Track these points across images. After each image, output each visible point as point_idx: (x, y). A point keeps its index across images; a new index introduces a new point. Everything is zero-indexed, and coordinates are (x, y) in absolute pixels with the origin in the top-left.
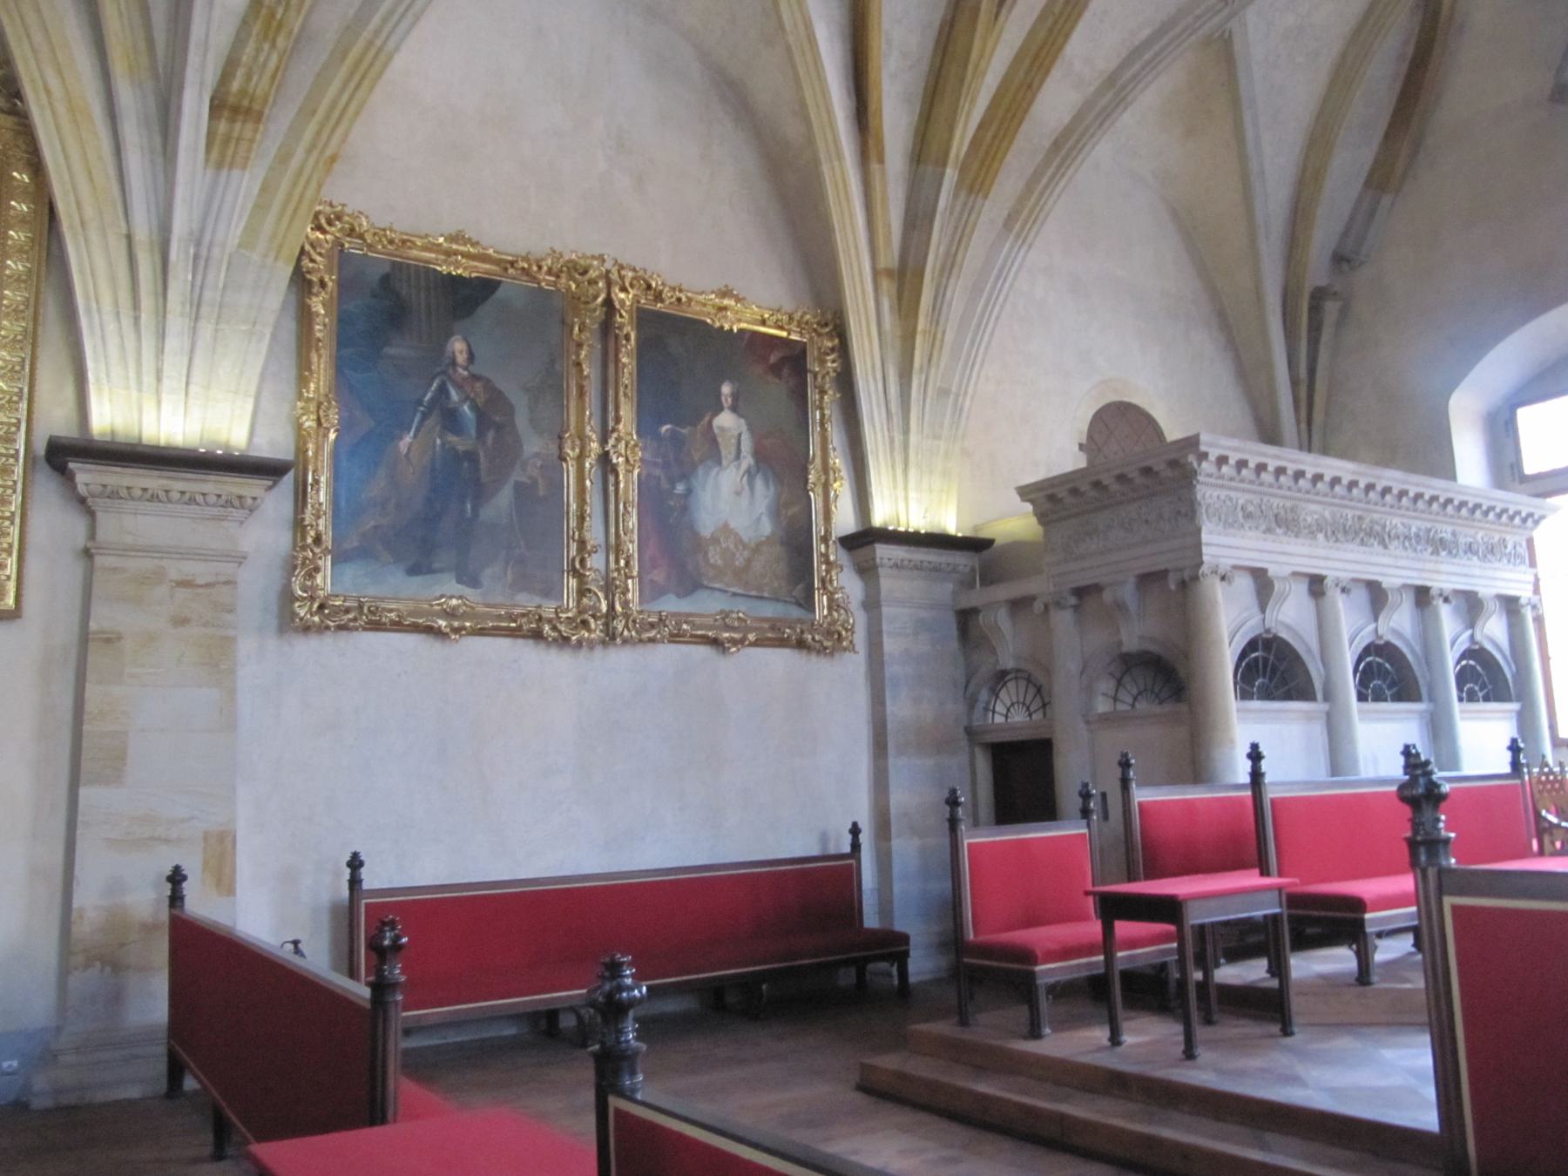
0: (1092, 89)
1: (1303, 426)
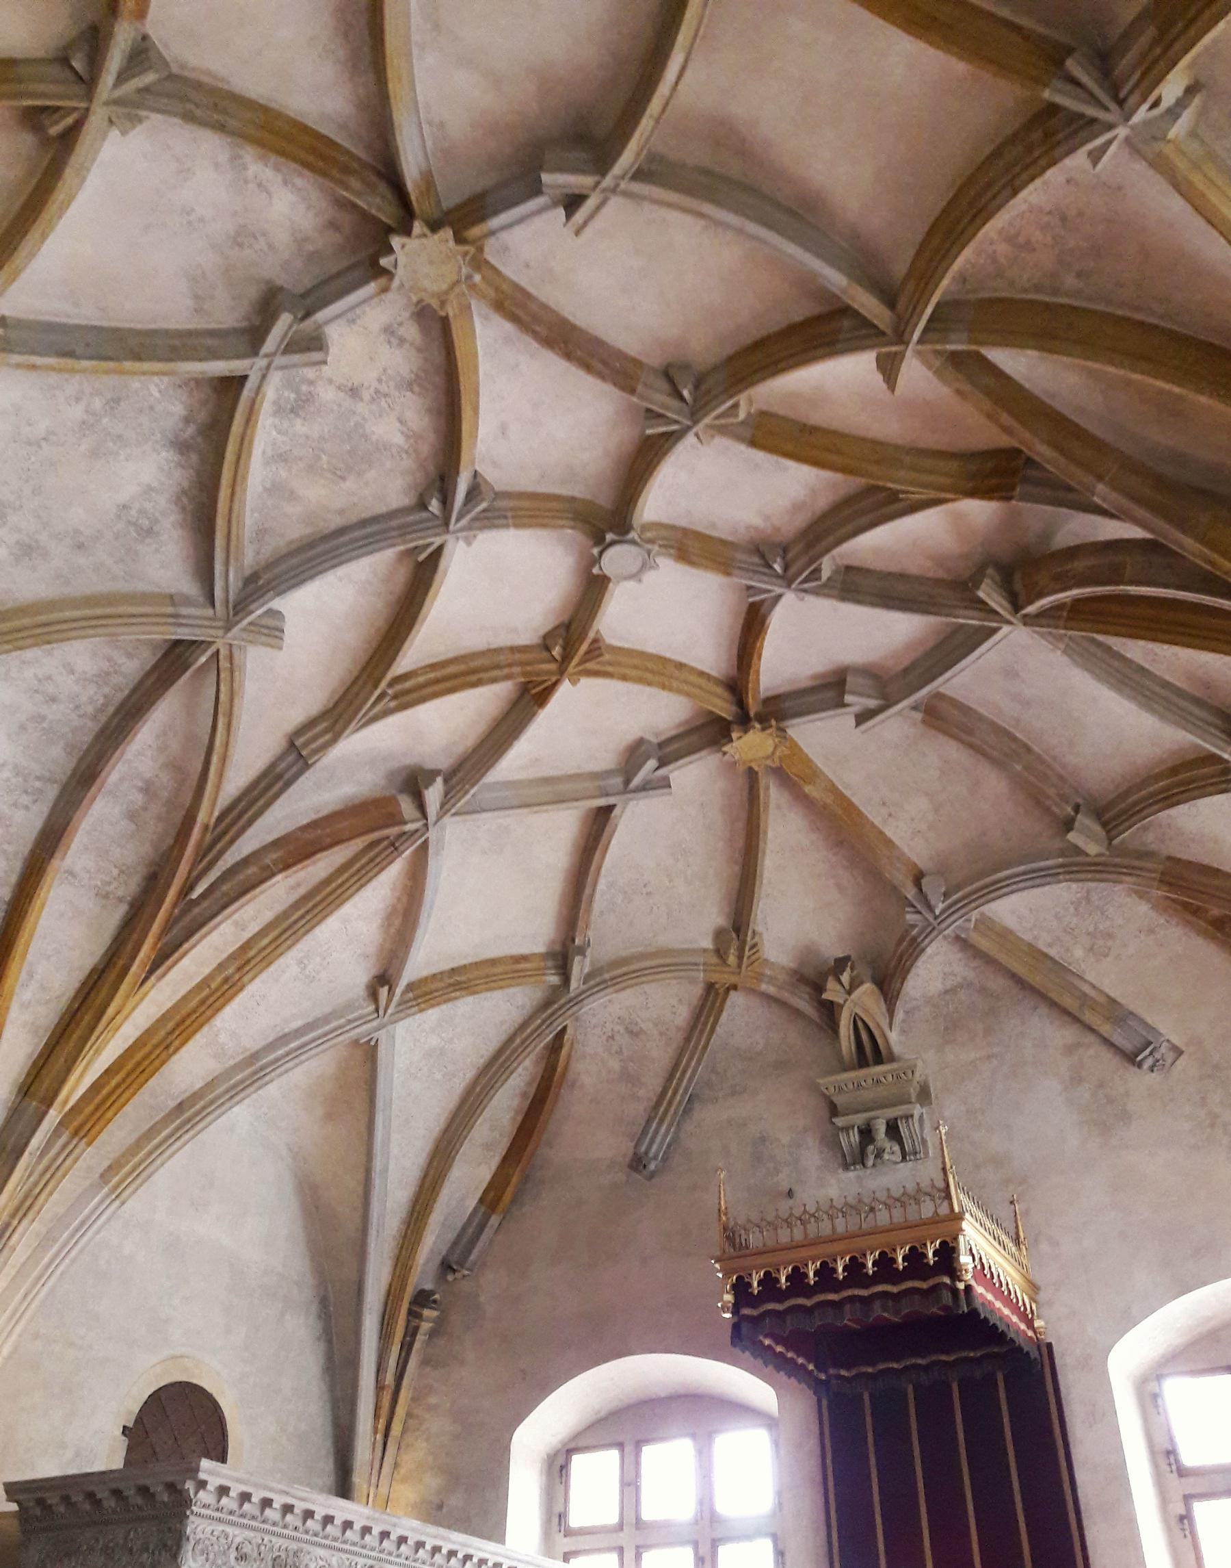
0: (232, 1062)
1: (379, 1437)
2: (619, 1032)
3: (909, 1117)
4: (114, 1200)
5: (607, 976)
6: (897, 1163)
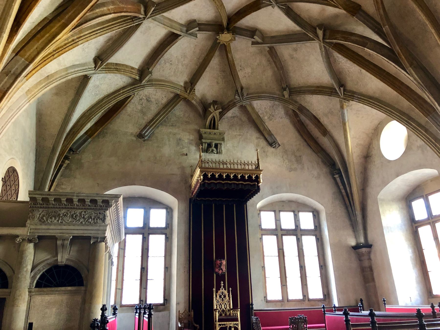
0: (61, 68)
2: (144, 99)
3: (221, 144)
4: (28, 102)
5: (153, 83)
6: (215, 153)
